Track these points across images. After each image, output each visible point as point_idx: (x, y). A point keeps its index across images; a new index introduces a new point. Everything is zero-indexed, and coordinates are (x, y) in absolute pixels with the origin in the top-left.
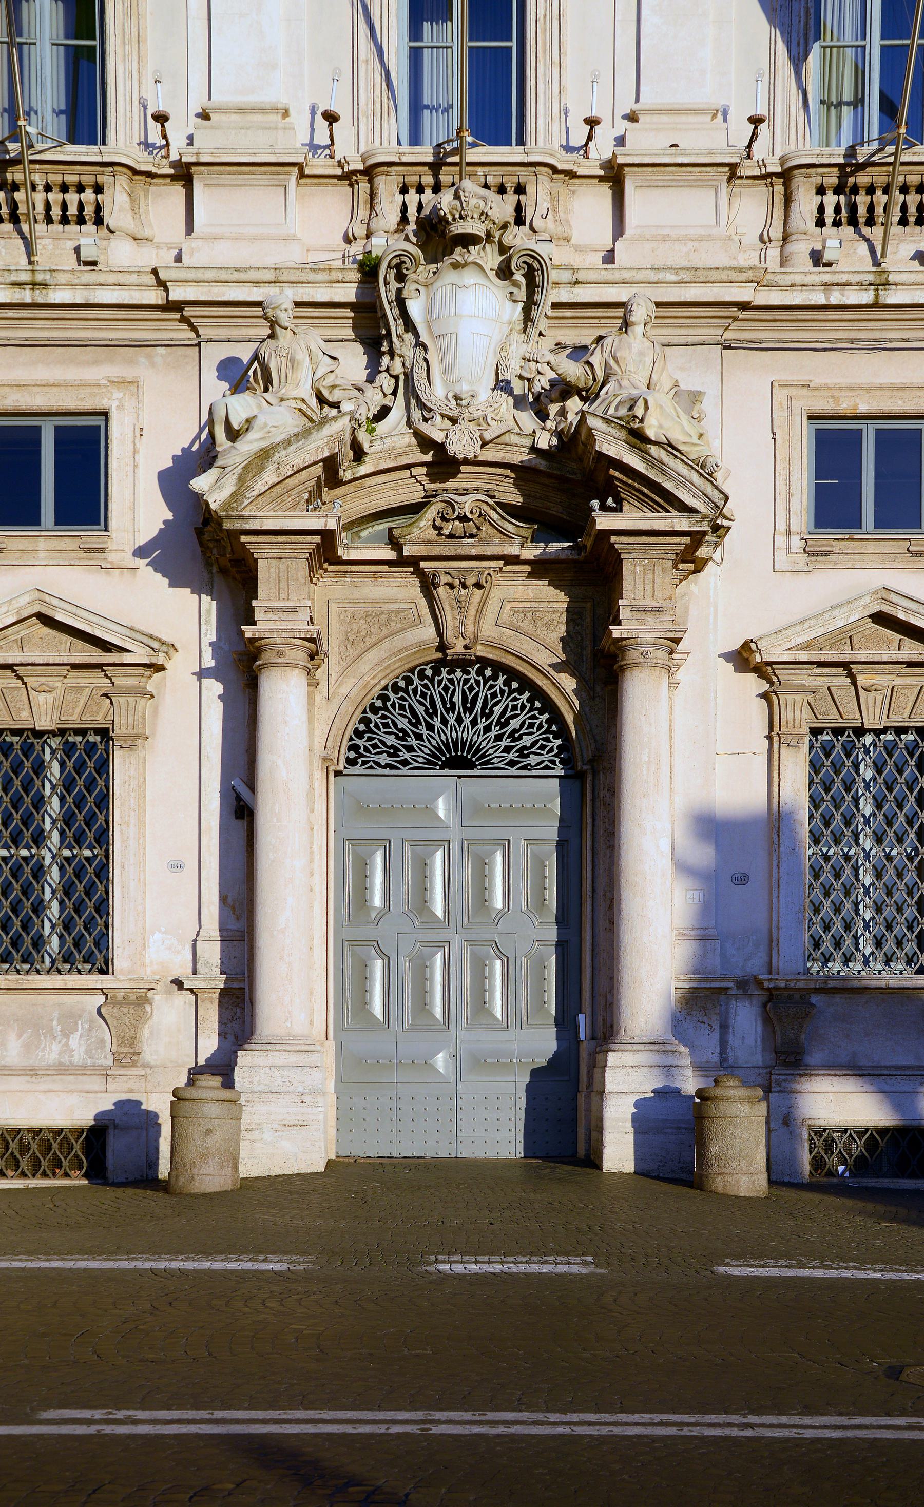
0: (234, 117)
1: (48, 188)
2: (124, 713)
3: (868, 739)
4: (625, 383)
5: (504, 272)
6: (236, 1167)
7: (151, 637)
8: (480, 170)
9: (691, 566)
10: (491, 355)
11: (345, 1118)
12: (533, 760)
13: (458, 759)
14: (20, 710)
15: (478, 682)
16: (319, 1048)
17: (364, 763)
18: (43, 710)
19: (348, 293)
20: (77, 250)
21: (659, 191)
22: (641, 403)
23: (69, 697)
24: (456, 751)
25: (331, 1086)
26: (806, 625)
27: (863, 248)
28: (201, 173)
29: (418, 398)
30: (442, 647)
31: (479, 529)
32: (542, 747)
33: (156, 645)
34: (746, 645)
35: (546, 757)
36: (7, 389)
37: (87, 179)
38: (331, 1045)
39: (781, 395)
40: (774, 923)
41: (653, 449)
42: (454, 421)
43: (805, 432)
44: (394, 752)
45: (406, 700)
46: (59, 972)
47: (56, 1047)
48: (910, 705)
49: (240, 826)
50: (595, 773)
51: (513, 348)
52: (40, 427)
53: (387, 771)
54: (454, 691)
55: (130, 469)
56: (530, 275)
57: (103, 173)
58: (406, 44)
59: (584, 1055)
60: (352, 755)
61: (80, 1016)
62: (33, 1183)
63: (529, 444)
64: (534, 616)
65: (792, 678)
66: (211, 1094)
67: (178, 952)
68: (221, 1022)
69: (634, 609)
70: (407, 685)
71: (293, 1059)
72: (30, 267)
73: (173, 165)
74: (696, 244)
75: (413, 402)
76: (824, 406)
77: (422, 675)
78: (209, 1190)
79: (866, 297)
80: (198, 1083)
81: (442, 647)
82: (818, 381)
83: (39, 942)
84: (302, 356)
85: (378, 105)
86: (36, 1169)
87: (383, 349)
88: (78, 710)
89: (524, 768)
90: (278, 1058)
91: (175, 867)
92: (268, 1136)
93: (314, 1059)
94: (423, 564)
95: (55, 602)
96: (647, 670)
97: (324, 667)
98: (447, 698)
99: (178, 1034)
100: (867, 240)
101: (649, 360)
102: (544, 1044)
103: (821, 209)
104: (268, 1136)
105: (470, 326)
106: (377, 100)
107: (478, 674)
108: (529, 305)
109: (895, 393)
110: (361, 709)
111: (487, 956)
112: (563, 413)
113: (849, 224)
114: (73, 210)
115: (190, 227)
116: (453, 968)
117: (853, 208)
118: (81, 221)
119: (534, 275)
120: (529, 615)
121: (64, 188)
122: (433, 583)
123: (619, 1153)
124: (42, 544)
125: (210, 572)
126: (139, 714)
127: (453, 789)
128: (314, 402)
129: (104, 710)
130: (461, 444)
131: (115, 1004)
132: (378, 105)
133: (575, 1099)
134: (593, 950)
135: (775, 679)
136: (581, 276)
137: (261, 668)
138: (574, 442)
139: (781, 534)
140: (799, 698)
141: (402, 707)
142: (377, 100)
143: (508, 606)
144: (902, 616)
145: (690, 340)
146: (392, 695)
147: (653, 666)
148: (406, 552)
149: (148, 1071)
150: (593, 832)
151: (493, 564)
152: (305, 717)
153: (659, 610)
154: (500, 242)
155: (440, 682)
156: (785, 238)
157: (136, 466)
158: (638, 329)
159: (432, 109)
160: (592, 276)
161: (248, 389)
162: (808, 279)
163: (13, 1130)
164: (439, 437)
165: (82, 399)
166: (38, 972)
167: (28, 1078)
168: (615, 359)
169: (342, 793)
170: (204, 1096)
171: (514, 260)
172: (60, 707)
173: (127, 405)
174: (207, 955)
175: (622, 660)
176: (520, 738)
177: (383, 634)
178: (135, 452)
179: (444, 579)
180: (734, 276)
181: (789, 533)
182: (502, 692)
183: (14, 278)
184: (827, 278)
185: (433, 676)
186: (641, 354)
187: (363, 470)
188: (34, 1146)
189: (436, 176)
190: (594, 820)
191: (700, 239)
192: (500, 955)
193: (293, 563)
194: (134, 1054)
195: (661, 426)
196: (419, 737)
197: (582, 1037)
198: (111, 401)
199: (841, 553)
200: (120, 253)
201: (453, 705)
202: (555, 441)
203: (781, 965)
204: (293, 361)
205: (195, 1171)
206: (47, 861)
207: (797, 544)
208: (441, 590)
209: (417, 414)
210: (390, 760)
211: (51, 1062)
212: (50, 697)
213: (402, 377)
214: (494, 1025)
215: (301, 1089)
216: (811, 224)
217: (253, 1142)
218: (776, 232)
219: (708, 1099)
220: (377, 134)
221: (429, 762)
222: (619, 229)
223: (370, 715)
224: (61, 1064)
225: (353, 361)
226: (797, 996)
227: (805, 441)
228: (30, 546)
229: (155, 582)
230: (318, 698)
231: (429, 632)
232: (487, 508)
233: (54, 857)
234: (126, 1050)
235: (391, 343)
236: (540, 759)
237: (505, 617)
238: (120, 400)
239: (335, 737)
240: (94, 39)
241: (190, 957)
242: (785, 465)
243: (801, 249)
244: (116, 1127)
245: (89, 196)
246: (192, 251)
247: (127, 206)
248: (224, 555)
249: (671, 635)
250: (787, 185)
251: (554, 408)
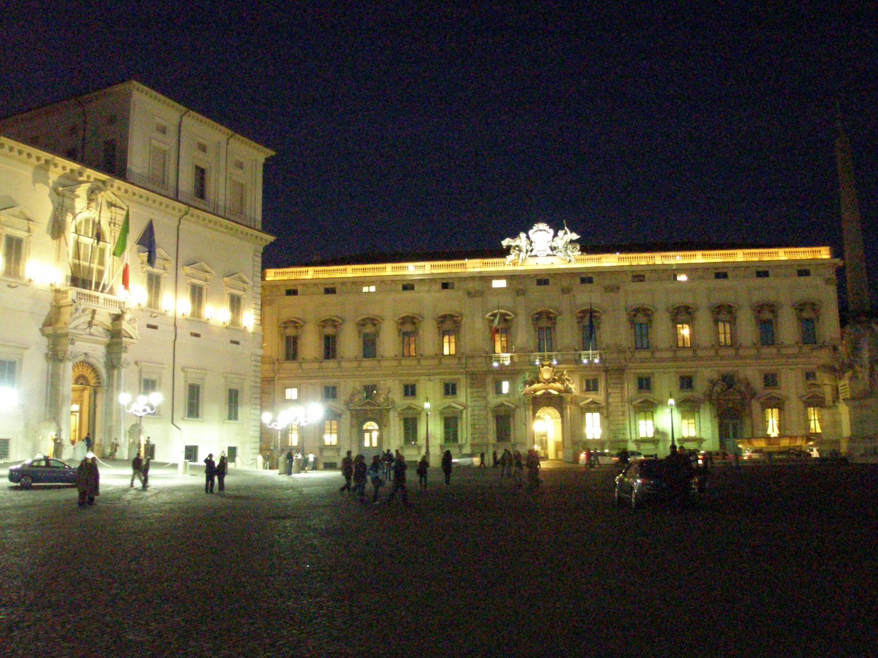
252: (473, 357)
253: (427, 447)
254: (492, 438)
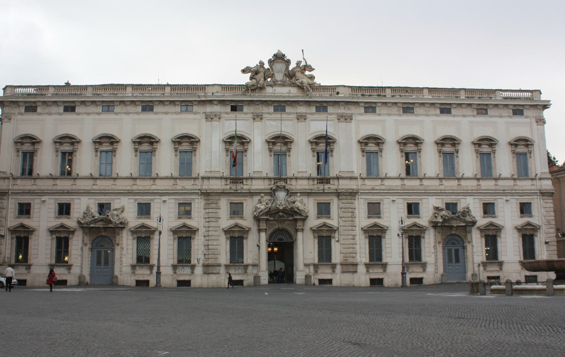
5: (285, 190)
105: (281, 195)
198: (244, 202)
200: (245, 187)
252: (209, 178)
253: (159, 267)
254: (224, 258)
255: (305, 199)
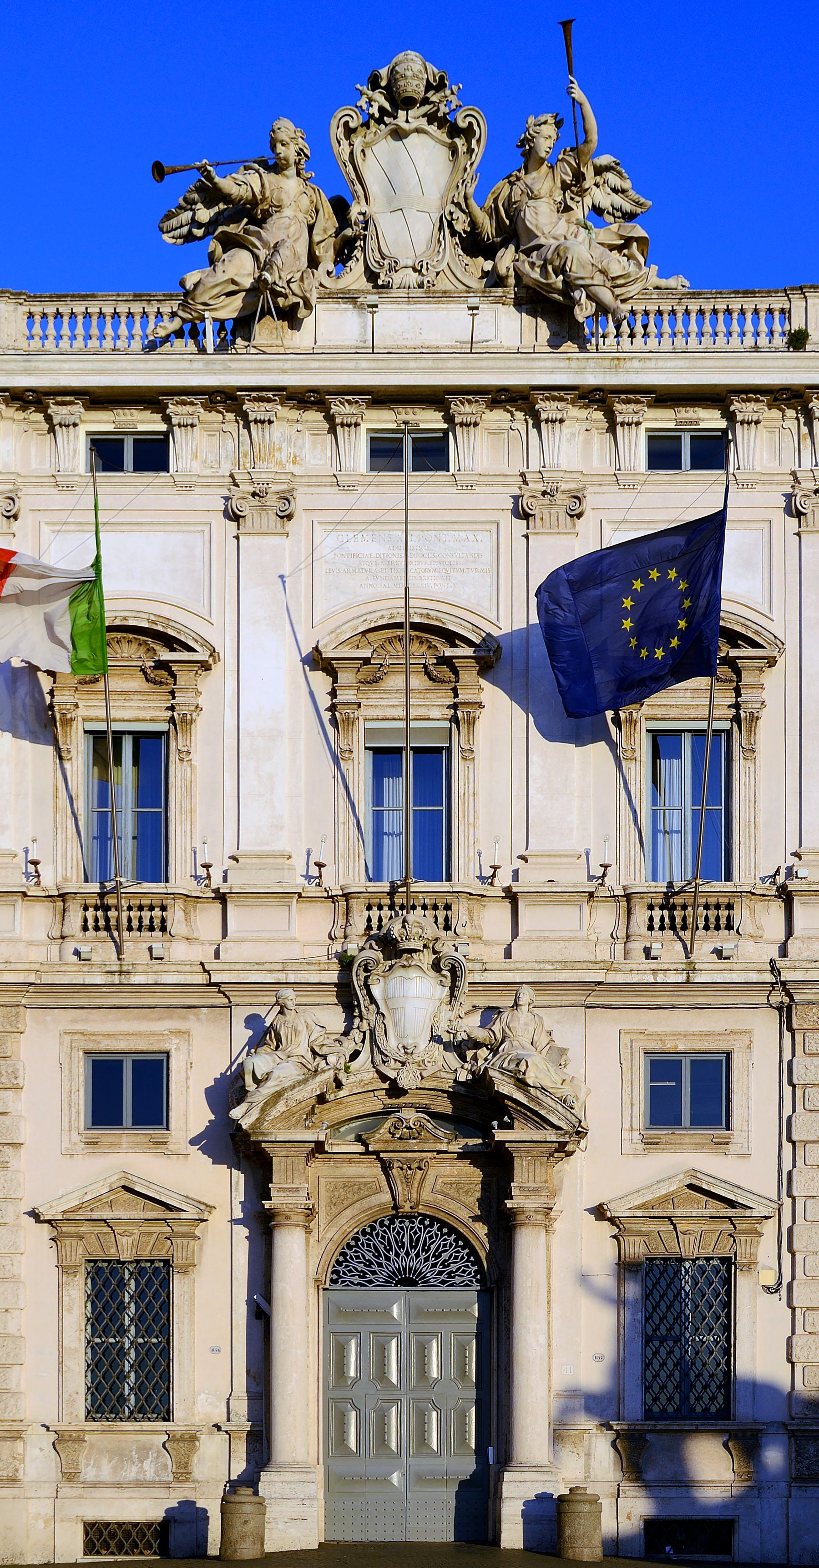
0: (254, 860)
1: (130, 908)
2: (180, 1249)
3: (687, 1265)
4: (515, 1043)
6: (262, 1544)
7: (200, 1202)
8: (420, 895)
9: (562, 1155)
10: (427, 1021)
11: (330, 1516)
12: (458, 1280)
13: (407, 1279)
14: (110, 1248)
15: (420, 1229)
16: (314, 1470)
17: (343, 1282)
18: (125, 1248)
19: (333, 976)
20: (150, 949)
21: (541, 908)
22: (523, 1063)
23: (143, 1239)
24: (405, 1274)
25: (321, 1495)
26: (640, 1193)
27: (679, 945)
28: (232, 898)
29: (379, 1048)
30: (395, 1207)
31: (419, 1134)
32: (464, 1271)
33: (203, 1207)
34: (601, 1205)
35: (466, 1278)
36: (101, 1037)
37: (156, 902)
38: (321, 1468)
39: (626, 1039)
40: (621, 1387)
41: (532, 1090)
42: (403, 1064)
43: (642, 1064)
44: (363, 1275)
45: (371, 1241)
46: (136, 1420)
47: (134, 1469)
48: (713, 1243)
49: (260, 1324)
50: (499, 1289)
51: (443, 1014)
52: (122, 1061)
53: (358, 1287)
54: (404, 1235)
55: (184, 1089)
56: (453, 970)
57: (167, 898)
58: (371, 808)
59: (492, 1474)
60: (335, 1277)
61: (151, 1449)
62: (120, 1558)
63: (453, 1078)
64: (457, 1186)
65: (633, 1226)
66: (247, 1499)
67: (217, 1407)
68: (248, 1453)
69: (521, 1189)
70: (372, 1231)
71: (298, 1477)
72: (119, 962)
73: (214, 891)
74: (566, 943)
75: (376, 1049)
76: (654, 1045)
77: (382, 1224)
78: (246, 1558)
79: (682, 978)
80: (239, 1492)
81: (395, 1207)
82: (651, 1029)
83: (122, 1400)
84: (302, 1027)
85: (351, 851)
86: (120, 1549)
87: (355, 1014)
88: (149, 1248)
89: (452, 1285)
90: (287, 1476)
91: (215, 1350)
92: (281, 1526)
93: (311, 1477)
94: (382, 1155)
95: (135, 1179)
96: (530, 1228)
97: (316, 1220)
98: (399, 1239)
99: (217, 1462)
100: (682, 940)
101: (531, 1029)
102: (468, 1466)
103: (651, 919)
104: (281, 1526)
105: (413, 1002)
106: (351, 848)
107: (420, 1223)
108: (453, 988)
109: (703, 1037)
110: (341, 1247)
111: (427, 1409)
112: (475, 1058)
113: (671, 929)
114: (146, 922)
115: (225, 934)
116: (404, 1417)
117: (672, 918)
118: (151, 928)
119: (455, 972)
120: (454, 1186)
121: (141, 908)
122: (389, 1166)
123: (512, 1535)
124: (124, 1139)
125: (238, 1157)
126: (190, 1250)
127: (403, 1299)
128: (309, 1055)
129: (167, 1247)
130: (407, 1080)
131: (175, 1441)
132: (351, 851)
133: (487, 1503)
134: (498, 1405)
135: (621, 1226)
136: (488, 966)
137: (275, 1226)
138: (481, 1081)
139: (626, 1130)
140: (637, 1239)
141: (369, 1245)
142: (351, 848)
143: (440, 1180)
144: (705, 1187)
145: (563, 1003)
146: (361, 1237)
147: (534, 1225)
148: (370, 1149)
149: (197, 1485)
150: (498, 1328)
151: (429, 1155)
152: (304, 1256)
153: (537, 1190)
154: (433, 947)
155: (394, 1229)
156: (628, 937)
157: (188, 1087)
158: (525, 1008)
159: (389, 834)
160: (496, 966)
161: (265, 1044)
162: (641, 967)
163: (105, 1523)
164: (392, 1074)
165: (152, 1044)
166: (121, 1420)
167: (116, 1489)
168: (508, 1027)
169: (328, 1302)
170: (243, 1500)
171: (443, 961)
172: (137, 1246)
173: (181, 1047)
174: (237, 1409)
175: (515, 1220)
176: (449, 1265)
177: (355, 1199)
178: (187, 1078)
179: (396, 1165)
180: (591, 966)
181: (631, 1129)
182: (437, 1235)
183: (108, 969)
184: (654, 966)
185: (390, 1225)
186: (526, 1024)
187: (342, 1094)
188: (120, 1534)
189: (392, 899)
190: (498, 1320)
191: (569, 940)
192: (436, 1408)
193: (296, 1160)
194: (187, 1473)
195: (536, 1077)
196: (380, 1265)
197: (491, 1463)
198: (171, 1045)
199: (667, 1143)
200: (179, 951)
201: (403, 1243)
202: (470, 1077)
203: (626, 1415)
204: (296, 1030)
205: (238, 1546)
206: (127, 1346)
207: (636, 1136)
208: (394, 1171)
209: (378, 1058)
210: (361, 1281)
211: (131, 1479)
212: (130, 1240)
213: (368, 1033)
214: (432, 1454)
215: (302, 1497)
216: (644, 930)
217: (271, 1529)
218: (622, 933)
219: (564, 1501)
220: (351, 870)
221: (387, 1281)
222: (515, 934)
223: (347, 1251)
224: (138, 1480)
225: (335, 1019)
226: (637, 1435)
227: (642, 1069)
228: (117, 1140)
229: (201, 1160)
230: (312, 1241)
231: (386, 1197)
232: (425, 1121)
233: (132, 1343)
234: (182, 1471)
235: (360, 1011)
236: (462, 1279)
237: (438, 1187)
238: (177, 1044)
239: (323, 1266)
240: (161, 807)
241: (225, 1410)
242: (629, 1085)
243: (637, 947)
244: (175, 1521)
245: (157, 913)
246: (227, 949)
247: (183, 919)
248: (249, 1150)
249: (546, 1206)
250: (628, 901)
251: (470, 1054)
255: (567, 1027)
